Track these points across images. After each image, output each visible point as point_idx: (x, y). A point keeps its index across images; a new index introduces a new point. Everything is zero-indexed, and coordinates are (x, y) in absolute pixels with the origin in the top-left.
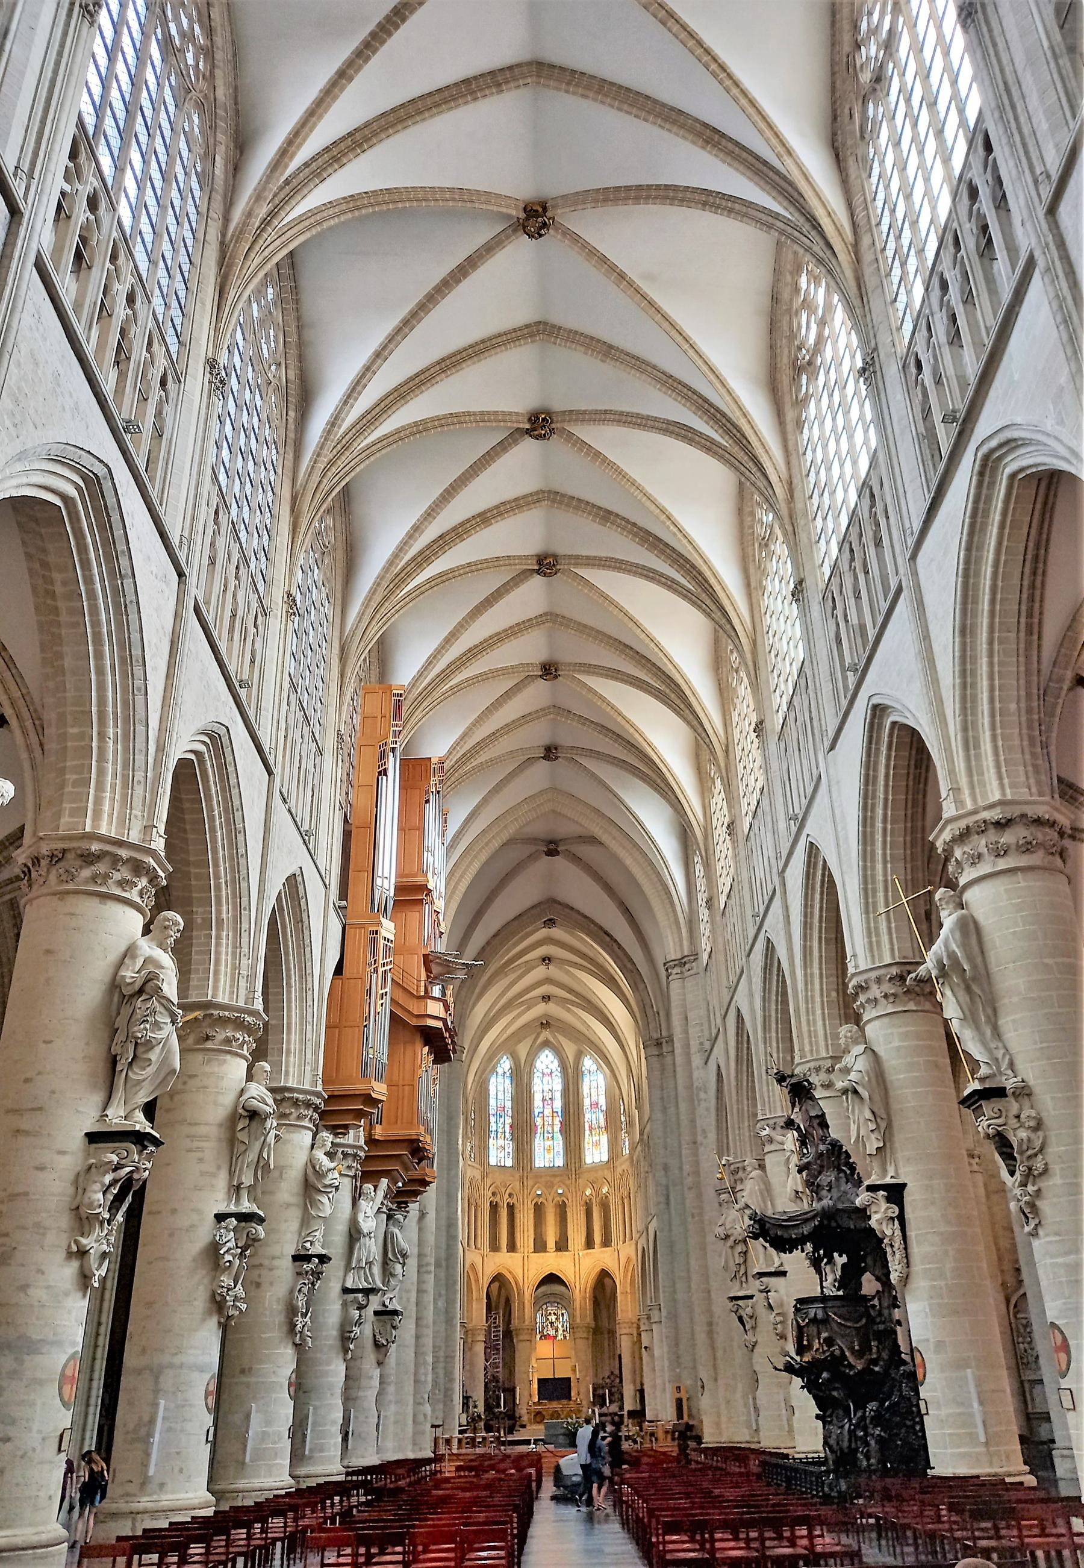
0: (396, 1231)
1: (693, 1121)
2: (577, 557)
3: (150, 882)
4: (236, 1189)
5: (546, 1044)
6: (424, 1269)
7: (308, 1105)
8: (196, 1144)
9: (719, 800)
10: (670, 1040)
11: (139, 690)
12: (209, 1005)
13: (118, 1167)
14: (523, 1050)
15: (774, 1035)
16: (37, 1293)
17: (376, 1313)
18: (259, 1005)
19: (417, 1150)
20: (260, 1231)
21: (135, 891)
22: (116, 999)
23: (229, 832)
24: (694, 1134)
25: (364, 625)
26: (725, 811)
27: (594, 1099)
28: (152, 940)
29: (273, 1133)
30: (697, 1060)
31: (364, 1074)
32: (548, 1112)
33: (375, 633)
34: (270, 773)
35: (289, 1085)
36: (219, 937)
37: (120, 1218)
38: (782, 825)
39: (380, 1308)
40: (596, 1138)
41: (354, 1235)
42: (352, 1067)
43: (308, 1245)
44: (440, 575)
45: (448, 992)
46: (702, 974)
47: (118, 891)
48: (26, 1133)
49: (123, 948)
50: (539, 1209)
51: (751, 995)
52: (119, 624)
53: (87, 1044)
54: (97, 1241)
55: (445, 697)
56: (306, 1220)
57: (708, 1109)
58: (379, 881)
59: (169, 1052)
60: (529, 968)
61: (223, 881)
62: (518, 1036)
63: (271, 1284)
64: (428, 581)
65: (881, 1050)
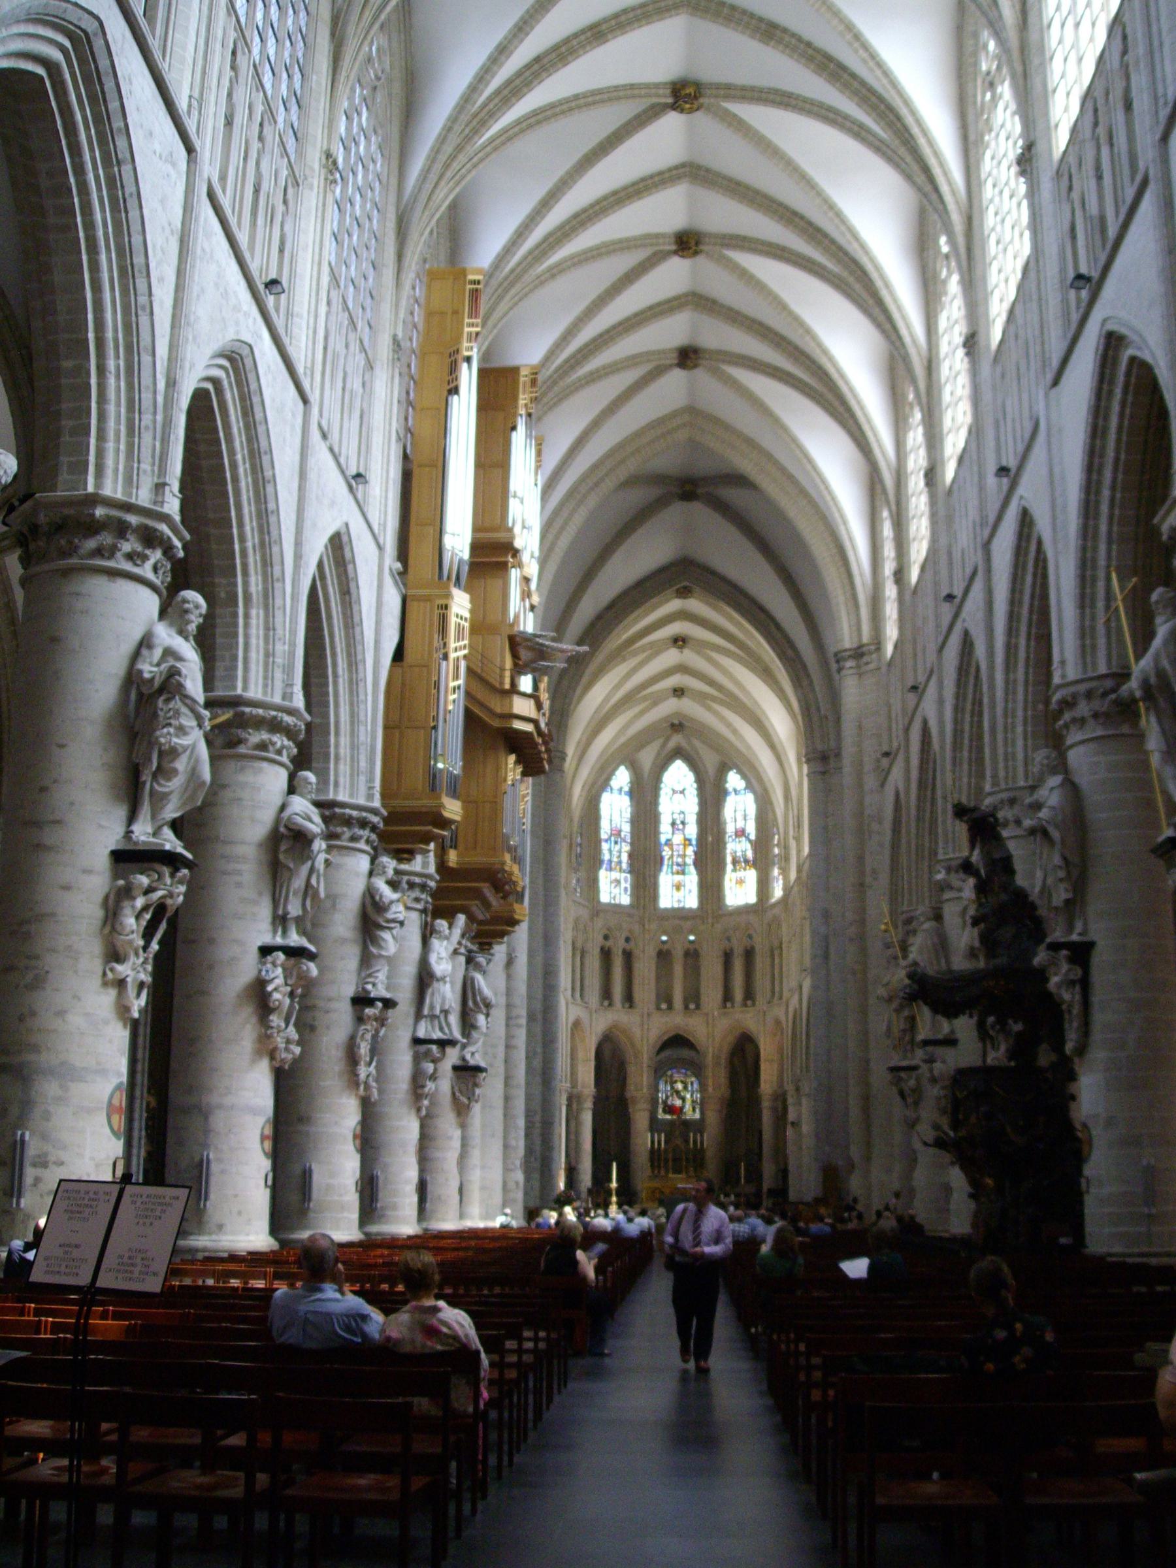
0: (478, 977)
1: (861, 859)
2: (728, 87)
3: (165, 553)
4: (280, 921)
5: (678, 753)
6: (513, 1022)
7: (363, 824)
8: (232, 866)
9: (916, 436)
10: (838, 755)
11: (143, 308)
12: (235, 702)
13: (149, 891)
14: (647, 758)
15: (966, 754)
16: (75, 1020)
17: (456, 1068)
18: (299, 701)
19: (500, 882)
20: (313, 969)
21: (149, 565)
22: (133, 696)
23: (255, 483)
24: (862, 873)
25: (429, 186)
26: (922, 452)
27: (740, 824)
28: (171, 625)
29: (321, 859)
30: (870, 782)
31: (433, 788)
32: (678, 839)
33: (444, 197)
34: (305, 401)
35: (342, 797)
36: (247, 616)
37: (155, 946)
38: (991, 480)
39: (459, 1063)
40: (741, 874)
41: (425, 978)
42: (416, 780)
43: (369, 987)
44: (535, 113)
45: (543, 686)
46: (884, 669)
47: (128, 566)
48: (48, 848)
49: (137, 635)
50: (663, 956)
51: (941, 701)
52: (117, 224)
53: (105, 749)
54: (133, 969)
55: (541, 281)
56: (366, 960)
57: (881, 845)
58: (449, 542)
59: (197, 761)
60: (657, 649)
61: (249, 544)
62: (642, 740)
63: (328, 1028)
64: (518, 122)
65: (1083, 779)
